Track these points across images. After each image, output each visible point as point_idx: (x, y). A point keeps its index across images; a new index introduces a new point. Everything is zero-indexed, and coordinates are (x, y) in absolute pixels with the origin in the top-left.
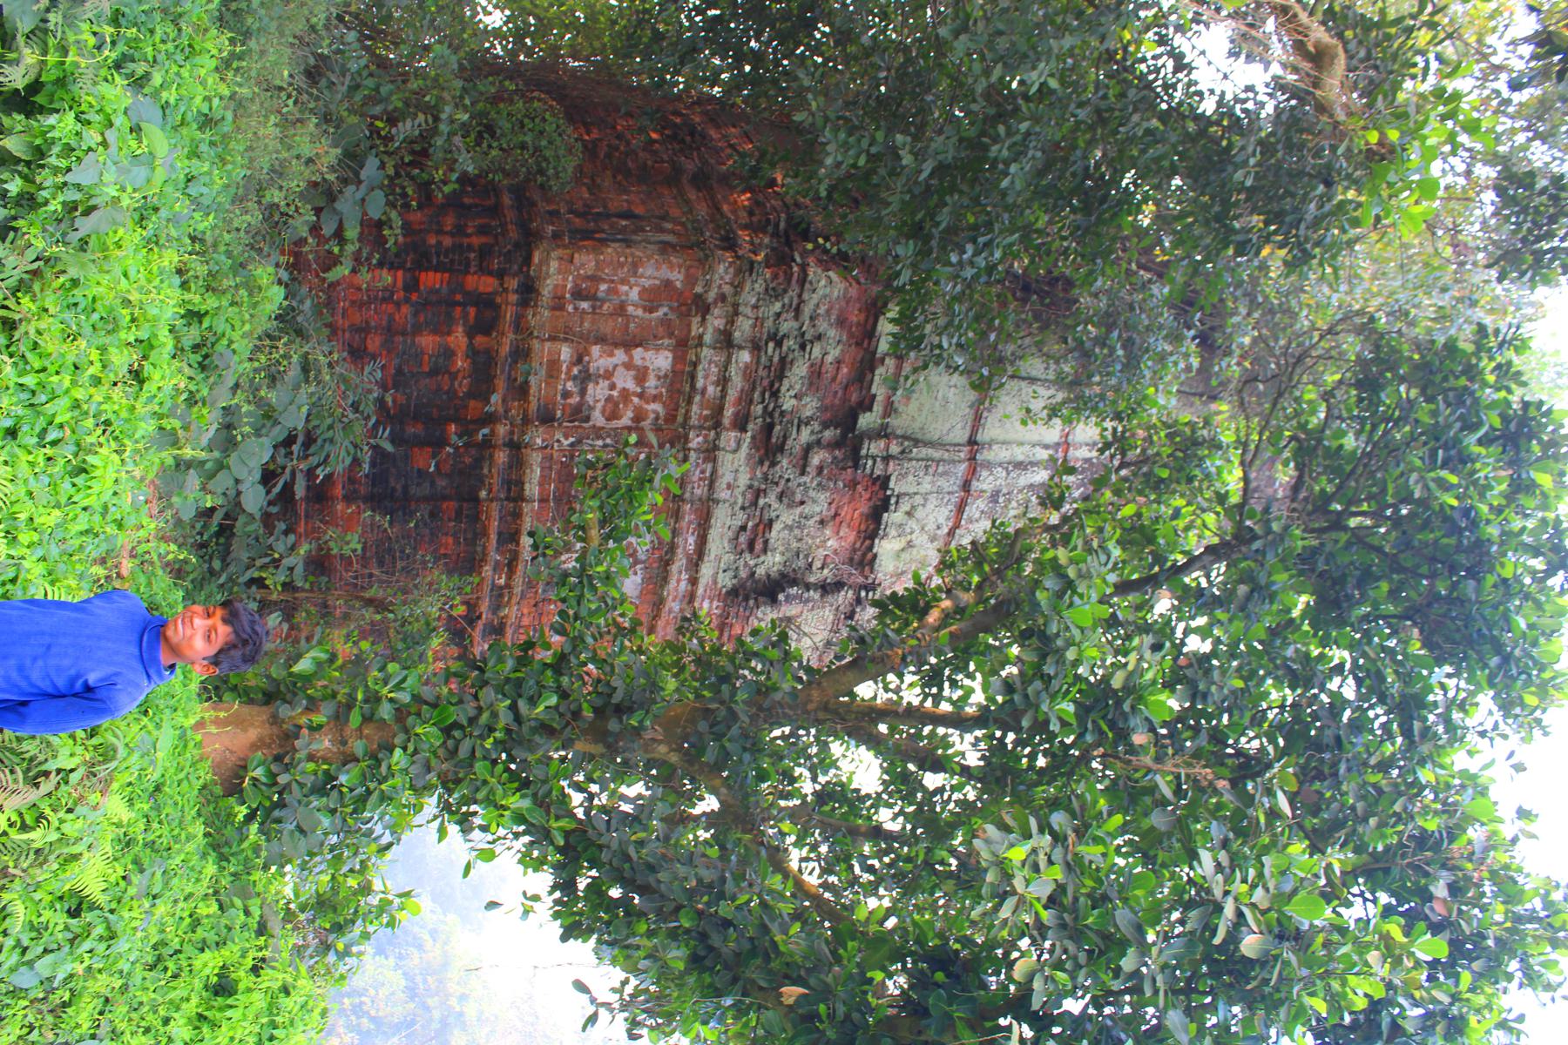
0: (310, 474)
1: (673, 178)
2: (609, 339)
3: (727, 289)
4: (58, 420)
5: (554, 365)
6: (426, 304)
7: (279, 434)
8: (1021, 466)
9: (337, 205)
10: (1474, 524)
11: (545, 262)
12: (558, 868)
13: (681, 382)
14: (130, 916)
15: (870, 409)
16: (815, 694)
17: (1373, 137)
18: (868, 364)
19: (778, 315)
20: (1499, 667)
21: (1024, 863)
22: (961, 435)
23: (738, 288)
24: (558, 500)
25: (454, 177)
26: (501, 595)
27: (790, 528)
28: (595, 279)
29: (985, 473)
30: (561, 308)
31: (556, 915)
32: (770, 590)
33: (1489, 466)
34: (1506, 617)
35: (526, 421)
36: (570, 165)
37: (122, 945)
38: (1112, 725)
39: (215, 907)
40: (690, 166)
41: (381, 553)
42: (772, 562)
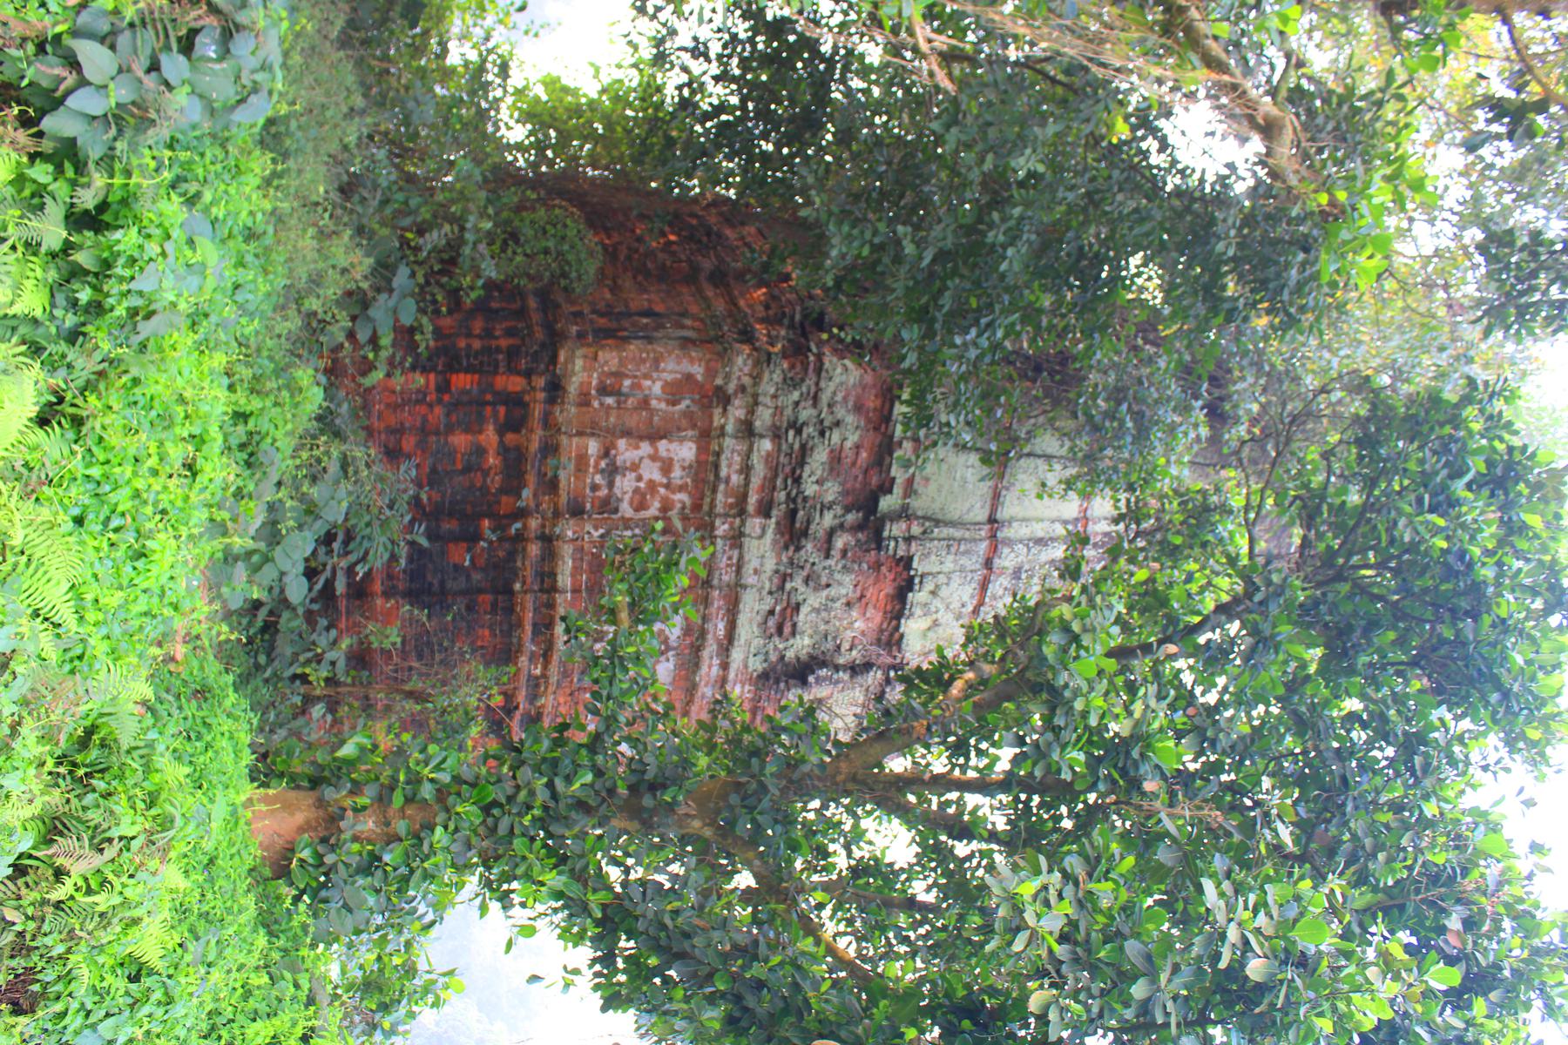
0: (350, 571)
1: (692, 278)
2: (635, 432)
3: (747, 380)
4: (120, 509)
5: (582, 459)
6: (456, 405)
7: (320, 528)
8: (1041, 542)
9: (371, 312)
10: (1470, 566)
11: (570, 359)
12: (597, 941)
13: (706, 472)
14: (186, 982)
15: (890, 491)
16: (843, 765)
17: (1324, 199)
18: (885, 449)
19: (797, 404)
20: (1500, 702)
21: (1035, 897)
22: (981, 514)
23: (756, 378)
24: (590, 590)
25: (480, 283)
26: (537, 686)
27: (817, 611)
28: (619, 375)
29: (1006, 550)
30: (587, 404)
31: (597, 987)
32: (801, 672)
33: (1479, 511)
34: (1505, 658)
35: (557, 514)
36: (591, 268)
37: (178, 1010)
38: (1124, 773)
39: (266, 979)
40: (707, 264)
41: (420, 646)
42: (801, 646)
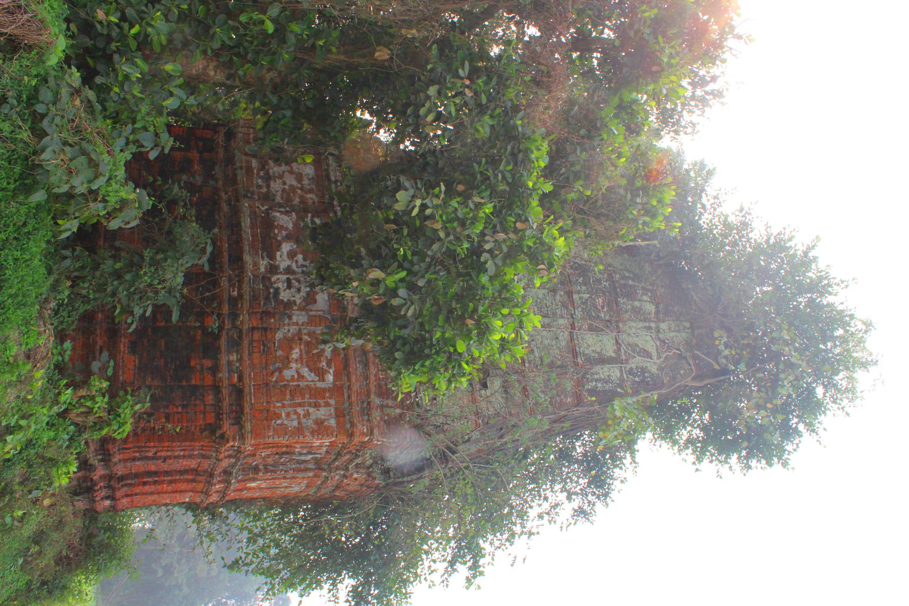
5: (249, 170)
26: (236, 305)
